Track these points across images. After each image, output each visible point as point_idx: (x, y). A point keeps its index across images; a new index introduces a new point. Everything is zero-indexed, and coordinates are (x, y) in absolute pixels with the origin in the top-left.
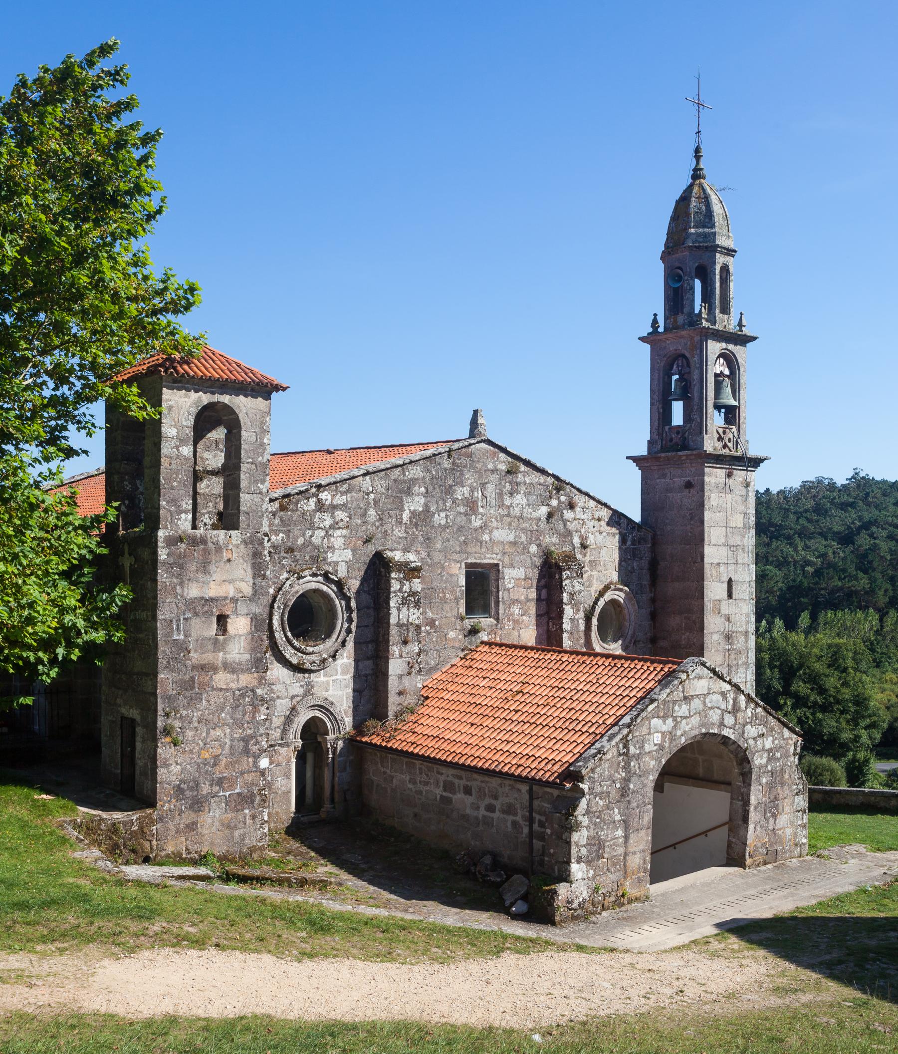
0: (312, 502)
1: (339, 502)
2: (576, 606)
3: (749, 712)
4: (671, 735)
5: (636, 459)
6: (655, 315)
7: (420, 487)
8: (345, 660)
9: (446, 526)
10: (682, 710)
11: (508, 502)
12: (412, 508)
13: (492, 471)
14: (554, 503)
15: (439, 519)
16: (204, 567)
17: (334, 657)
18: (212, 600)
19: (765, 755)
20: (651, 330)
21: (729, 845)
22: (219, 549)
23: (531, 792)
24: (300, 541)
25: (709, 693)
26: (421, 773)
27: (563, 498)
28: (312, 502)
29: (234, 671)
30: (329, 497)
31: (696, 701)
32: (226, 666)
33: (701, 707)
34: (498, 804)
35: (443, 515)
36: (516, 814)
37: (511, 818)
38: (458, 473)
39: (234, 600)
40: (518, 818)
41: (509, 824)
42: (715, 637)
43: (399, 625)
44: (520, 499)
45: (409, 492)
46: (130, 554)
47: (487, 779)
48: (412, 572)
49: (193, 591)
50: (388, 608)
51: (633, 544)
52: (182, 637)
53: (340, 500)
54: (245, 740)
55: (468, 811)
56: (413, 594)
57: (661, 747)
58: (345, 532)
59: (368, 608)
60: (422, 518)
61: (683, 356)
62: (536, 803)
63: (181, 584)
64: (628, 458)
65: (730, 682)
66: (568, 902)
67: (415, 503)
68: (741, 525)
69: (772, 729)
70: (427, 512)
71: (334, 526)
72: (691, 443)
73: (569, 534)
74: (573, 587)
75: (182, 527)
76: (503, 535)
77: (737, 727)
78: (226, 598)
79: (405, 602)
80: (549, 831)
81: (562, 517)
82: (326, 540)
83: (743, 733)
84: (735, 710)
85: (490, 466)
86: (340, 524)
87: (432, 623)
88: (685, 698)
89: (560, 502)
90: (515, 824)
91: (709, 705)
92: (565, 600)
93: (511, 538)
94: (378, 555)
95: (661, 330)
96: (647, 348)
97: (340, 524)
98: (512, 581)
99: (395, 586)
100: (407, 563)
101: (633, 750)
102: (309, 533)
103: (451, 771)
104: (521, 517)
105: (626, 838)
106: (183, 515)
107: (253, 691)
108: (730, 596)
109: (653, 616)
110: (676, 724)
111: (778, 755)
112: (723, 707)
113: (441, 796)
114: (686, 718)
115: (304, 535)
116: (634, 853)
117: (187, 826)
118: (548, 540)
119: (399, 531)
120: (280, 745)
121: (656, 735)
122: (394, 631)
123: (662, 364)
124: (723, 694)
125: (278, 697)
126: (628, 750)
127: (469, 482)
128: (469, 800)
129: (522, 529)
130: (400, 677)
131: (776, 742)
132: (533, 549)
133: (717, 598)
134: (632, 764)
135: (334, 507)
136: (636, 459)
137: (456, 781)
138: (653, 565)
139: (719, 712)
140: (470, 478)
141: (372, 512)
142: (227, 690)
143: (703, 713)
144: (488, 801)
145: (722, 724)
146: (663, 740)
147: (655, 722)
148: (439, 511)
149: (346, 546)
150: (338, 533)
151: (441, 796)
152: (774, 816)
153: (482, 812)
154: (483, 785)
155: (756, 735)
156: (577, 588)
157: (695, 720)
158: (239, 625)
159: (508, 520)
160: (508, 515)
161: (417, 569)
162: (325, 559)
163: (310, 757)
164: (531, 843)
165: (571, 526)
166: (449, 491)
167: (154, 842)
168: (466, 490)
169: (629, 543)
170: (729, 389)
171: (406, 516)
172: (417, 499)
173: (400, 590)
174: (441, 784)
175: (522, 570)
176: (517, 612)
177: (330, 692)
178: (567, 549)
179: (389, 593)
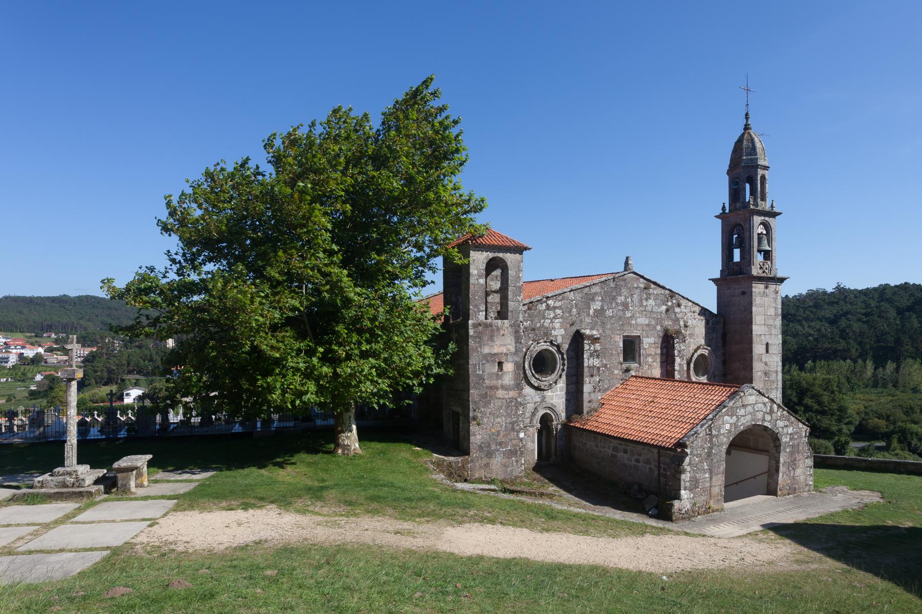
0: (544, 305)
2: (682, 358)
3: (779, 414)
4: (735, 425)
5: (714, 280)
6: (724, 204)
8: (561, 385)
9: (613, 317)
10: (742, 412)
11: (645, 304)
12: (595, 308)
13: (636, 288)
14: (670, 304)
15: (609, 313)
16: (491, 338)
17: (556, 383)
18: (495, 354)
20: (721, 212)
21: (768, 484)
22: (498, 329)
23: (659, 453)
24: (538, 325)
26: (601, 442)
27: (674, 301)
28: (544, 305)
29: (506, 390)
30: (553, 303)
31: (749, 407)
32: (503, 387)
33: (752, 411)
34: (641, 458)
35: (611, 311)
36: (651, 464)
37: (649, 466)
38: (618, 290)
39: (506, 354)
40: (652, 466)
41: (648, 469)
42: (759, 374)
43: (588, 367)
44: (651, 302)
45: (593, 300)
46: (456, 332)
47: (636, 446)
48: (595, 340)
49: (486, 350)
50: (583, 358)
51: (713, 325)
52: (481, 373)
53: (558, 304)
54: (513, 423)
55: (626, 462)
56: (596, 351)
57: (730, 431)
58: (560, 320)
59: (573, 358)
60: (600, 313)
61: (740, 225)
62: (662, 458)
63: (480, 347)
64: (709, 279)
65: (768, 398)
66: (680, 510)
67: (596, 305)
68: (774, 314)
69: (792, 423)
71: (555, 317)
72: (745, 271)
73: (677, 320)
74: (680, 347)
75: (480, 319)
76: (643, 321)
77: (772, 421)
78: (502, 353)
79: (591, 355)
80: (669, 473)
83: (776, 424)
84: (771, 412)
85: (635, 285)
86: (558, 316)
87: (605, 366)
88: (743, 405)
89: (673, 303)
90: (650, 469)
92: (676, 354)
93: (647, 322)
94: (578, 332)
95: (727, 211)
96: (720, 221)
97: (558, 316)
99: (586, 347)
100: (592, 336)
101: (714, 432)
102: (542, 321)
103: (617, 441)
104: (652, 311)
105: (711, 478)
106: (481, 313)
107: (516, 399)
108: (767, 352)
109: (724, 362)
110: (738, 419)
111: (796, 437)
112: (764, 410)
113: (612, 454)
114: (743, 416)
115: (540, 322)
116: (715, 486)
117: (485, 465)
118: (666, 323)
120: (529, 426)
121: (727, 425)
122: (586, 370)
123: (728, 229)
124: (764, 404)
125: (528, 403)
126: (712, 432)
128: (626, 456)
129: (652, 318)
130: (590, 393)
131: (795, 430)
132: (659, 328)
133: (760, 353)
134: (714, 440)
135: (555, 308)
136: (714, 280)
137: (619, 447)
138: (724, 336)
139: (762, 413)
140: (625, 292)
141: (574, 310)
142: (503, 399)
143: (753, 414)
144: (636, 457)
145: (764, 420)
146: (731, 427)
147: (726, 417)
148: (609, 309)
149: (561, 327)
150: (557, 321)
151: (612, 454)
152: (794, 469)
153: (633, 462)
154: (633, 449)
156: (682, 348)
157: (749, 418)
158: (509, 367)
159: (645, 313)
160: (645, 311)
161: (598, 339)
162: (551, 334)
163: (544, 433)
164: (659, 479)
165: (679, 316)
166: (614, 298)
167: (469, 472)
168: (623, 298)
169: (710, 324)
170: (766, 241)
171: (591, 312)
172: (597, 303)
173: (589, 349)
174: (611, 448)
175: (653, 339)
177: (554, 400)
178: (677, 327)
179: (583, 351)
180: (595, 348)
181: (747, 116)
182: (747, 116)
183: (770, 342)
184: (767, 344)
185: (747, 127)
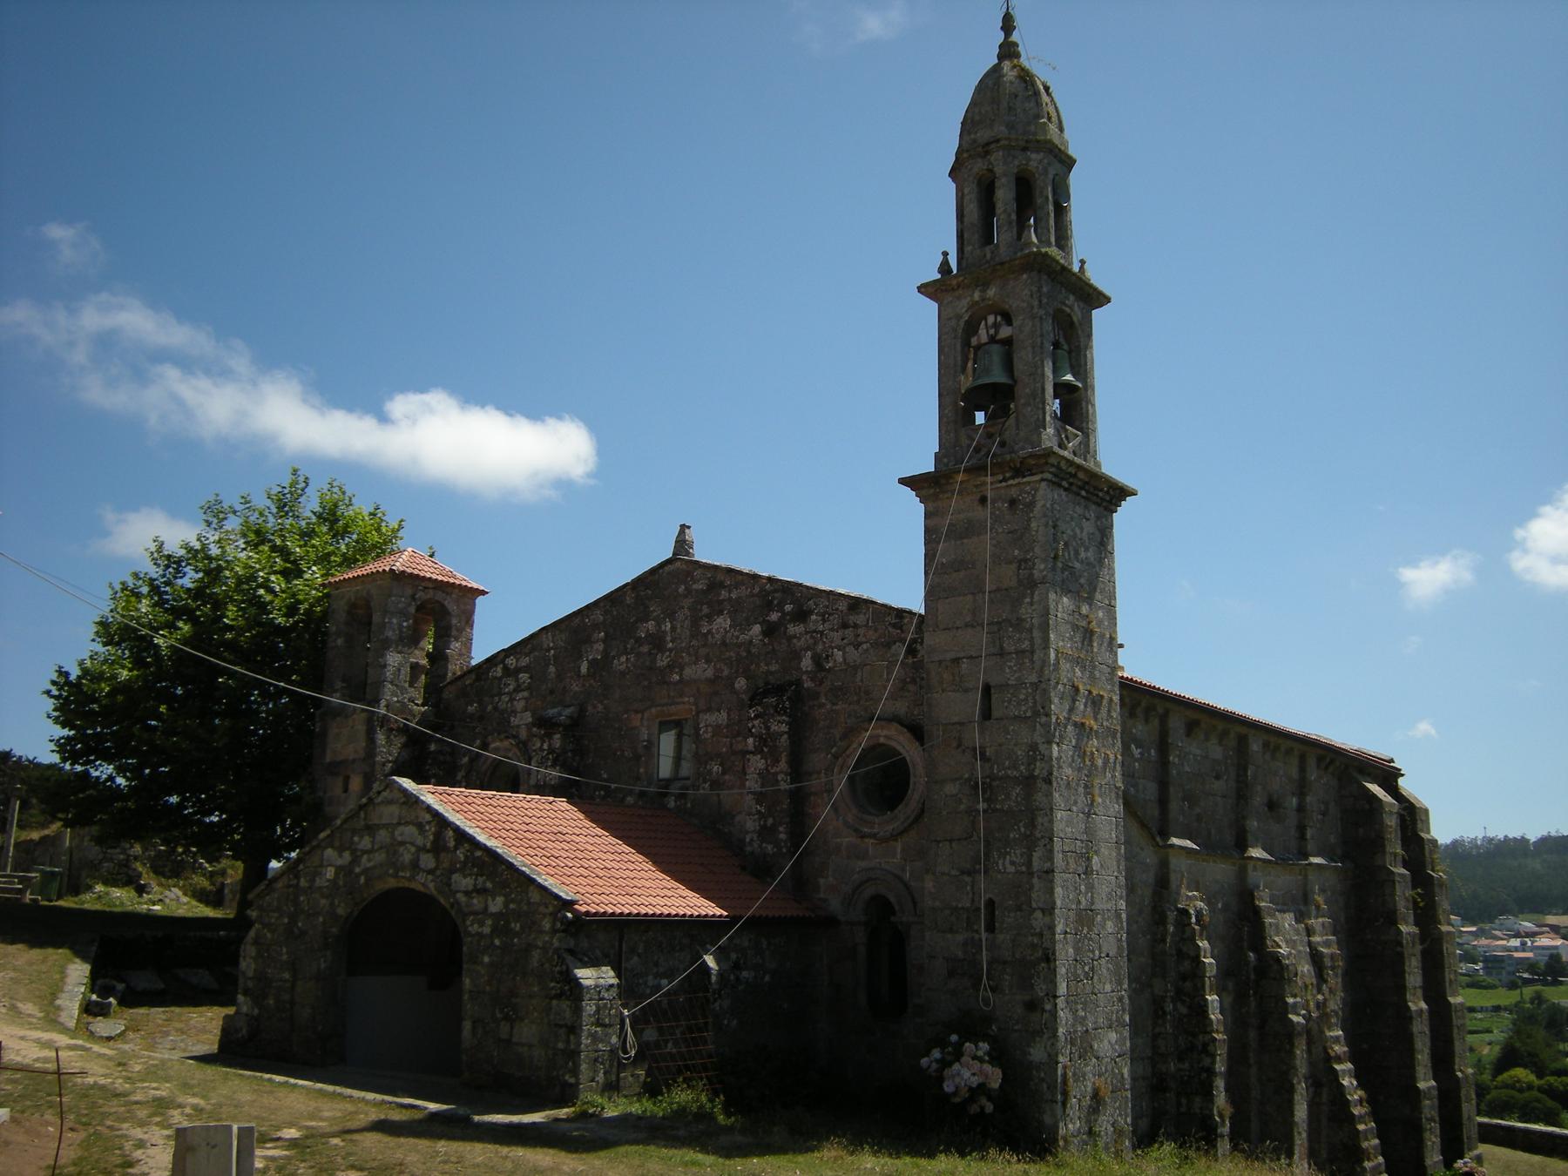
0: (499, 669)
1: (523, 664)
10: (366, 843)
12: (590, 657)
14: (774, 617)
19: (489, 922)
28: (499, 669)
33: (388, 840)
44: (723, 622)
45: (588, 641)
53: (525, 661)
57: (334, 882)
58: (526, 694)
67: (596, 651)
70: (607, 656)
71: (518, 689)
74: (768, 728)
77: (438, 873)
81: (785, 633)
82: (509, 705)
83: (449, 885)
91: (399, 839)
93: (710, 673)
98: (710, 729)
104: (724, 643)
108: (987, 714)
110: (355, 860)
112: (420, 841)
118: (764, 668)
119: (577, 685)
121: (329, 869)
127: (655, 614)
134: (302, 899)
135: (518, 670)
145: (415, 865)
147: (329, 852)
150: (520, 695)
155: (471, 888)
171: (584, 668)
173: (541, 749)
180: (550, 745)
181: (1008, 24)
182: (1008, 24)
183: (992, 684)
185: (1008, 51)
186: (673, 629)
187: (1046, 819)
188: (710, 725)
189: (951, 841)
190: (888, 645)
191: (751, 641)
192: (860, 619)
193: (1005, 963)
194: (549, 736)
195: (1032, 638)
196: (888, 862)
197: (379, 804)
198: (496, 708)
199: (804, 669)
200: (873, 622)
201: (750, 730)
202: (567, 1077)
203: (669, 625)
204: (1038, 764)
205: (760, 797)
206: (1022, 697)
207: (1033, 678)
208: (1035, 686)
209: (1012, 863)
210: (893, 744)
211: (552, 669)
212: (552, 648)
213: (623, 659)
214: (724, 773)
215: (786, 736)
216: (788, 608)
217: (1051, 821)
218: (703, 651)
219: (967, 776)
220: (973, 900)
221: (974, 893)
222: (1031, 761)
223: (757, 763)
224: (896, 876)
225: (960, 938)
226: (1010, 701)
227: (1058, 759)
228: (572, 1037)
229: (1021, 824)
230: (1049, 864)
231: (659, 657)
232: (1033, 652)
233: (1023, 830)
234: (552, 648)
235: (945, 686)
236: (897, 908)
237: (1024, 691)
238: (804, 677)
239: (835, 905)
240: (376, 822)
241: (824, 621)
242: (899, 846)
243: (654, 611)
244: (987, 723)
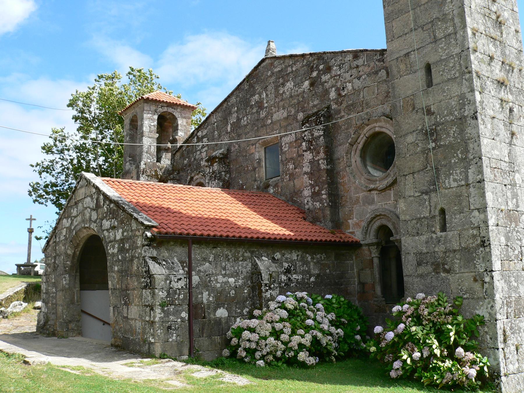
7: (234, 108)
12: (232, 122)
25: (85, 198)
44: (290, 85)
45: (230, 113)
53: (205, 132)
70: (239, 120)
74: (312, 135)
89: (319, 71)
93: (285, 115)
98: (287, 145)
108: (430, 83)
110: (72, 221)
124: (91, 196)
150: (204, 150)
155: (109, 227)
157: (79, 218)
171: (229, 129)
173: (209, 173)
176: (291, 167)
184: (428, 68)
186: (267, 95)
187: (476, 144)
188: (288, 143)
189: (413, 173)
190: (376, 73)
191: (304, 91)
192: (360, 62)
193: (455, 251)
194: (212, 165)
195: (454, 24)
196: (387, 204)
197: (78, 189)
198: (195, 159)
199: (331, 98)
200: (367, 62)
201: (303, 139)
202: (151, 339)
203: (265, 94)
204: (466, 107)
205: (311, 175)
206: (451, 65)
207: (457, 50)
208: (459, 55)
209: (455, 180)
210: (384, 130)
211: (216, 133)
212: (216, 122)
213: (245, 119)
214: (295, 168)
215: (322, 137)
216: (321, 67)
217: (479, 145)
218: (281, 104)
219: (420, 128)
220: (430, 211)
221: (430, 206)
222: (462, 106)
223: (308, 156)
224: (391, 211)
225: (424, 238)
226: (443, 71)
227: (482, 102)
228: (152, 312)
229: (459, 152)
230: (480, 176)
231: (261, 113)
232: (456, 33)
233: (460, 155)
234: (216, 122)
235: (401, 73)
236: (393, 231)
237: (453, 61)
238: (332, 103)
239: (358, 236)
240: (78, 200)
241: (340, 68)
242: (392, 192)
243: (258, 89)
244: (430, 89)
